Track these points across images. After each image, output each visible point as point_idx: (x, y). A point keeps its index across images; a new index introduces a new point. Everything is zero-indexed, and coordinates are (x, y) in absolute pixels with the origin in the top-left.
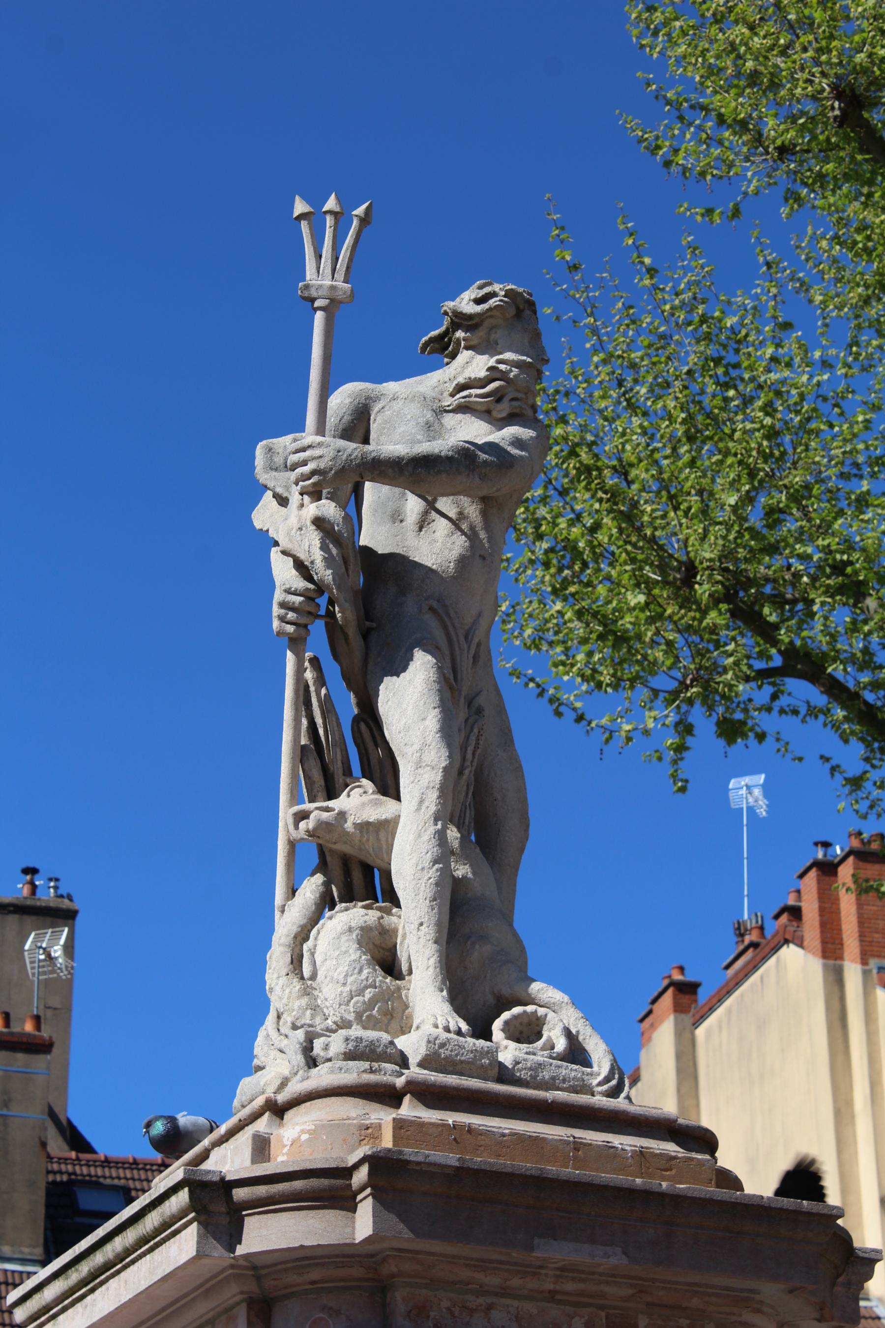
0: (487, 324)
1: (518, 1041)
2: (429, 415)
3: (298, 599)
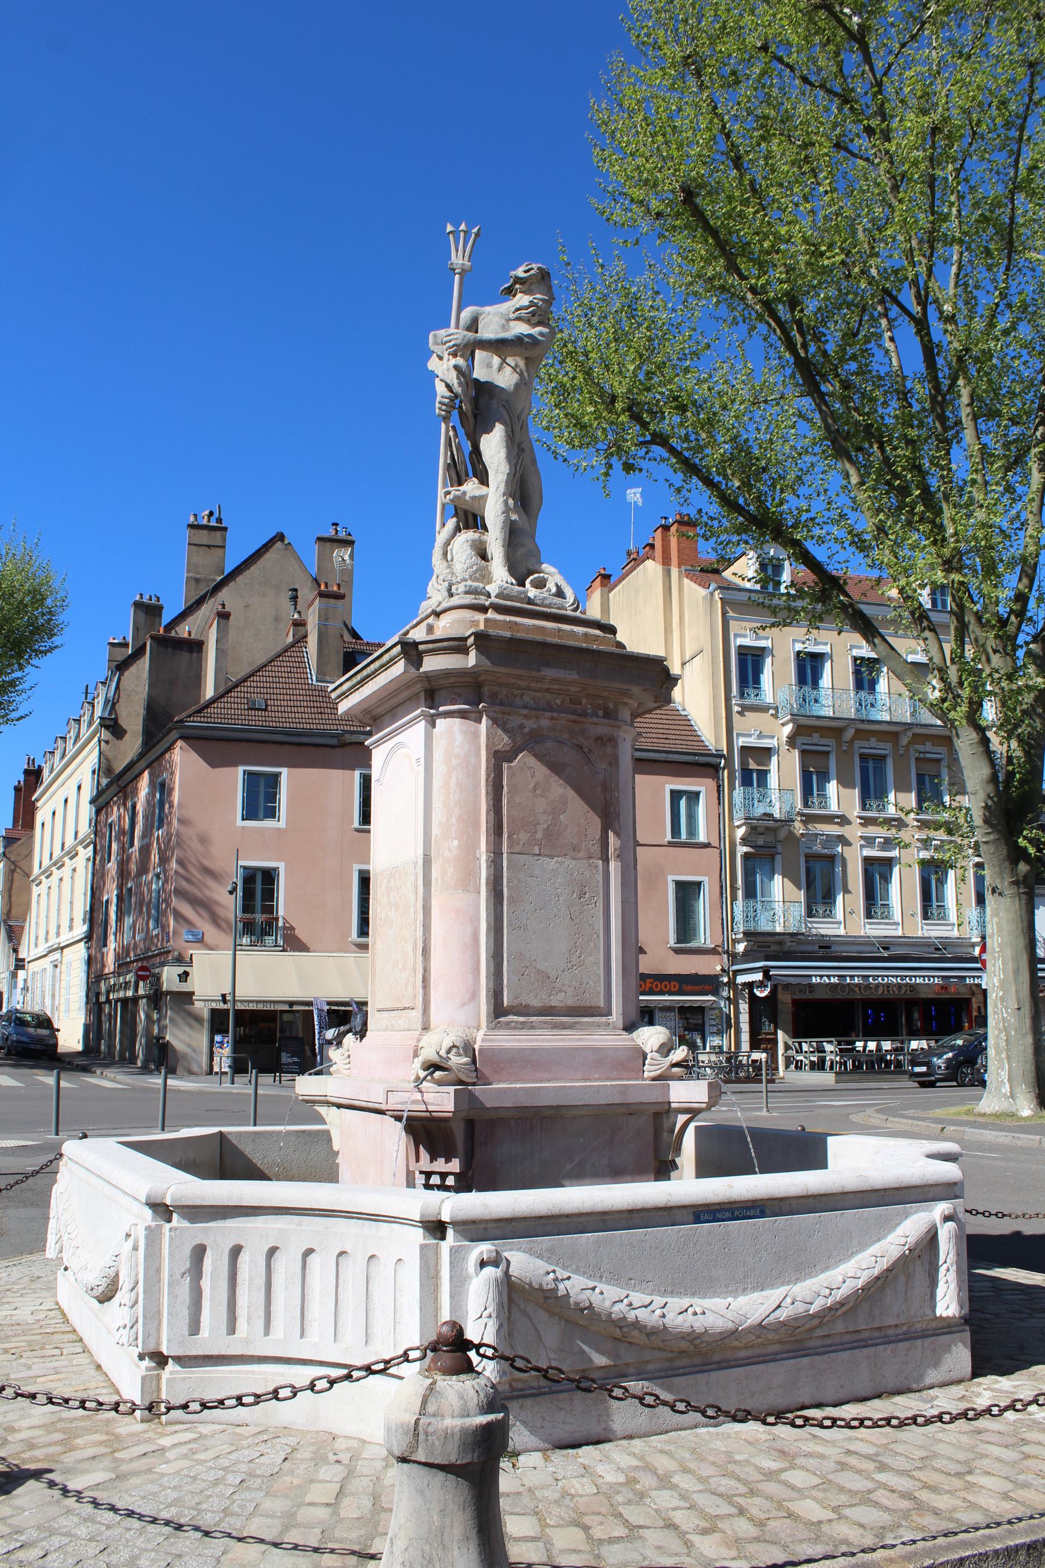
2: (504, 322)
3: (447, 401)
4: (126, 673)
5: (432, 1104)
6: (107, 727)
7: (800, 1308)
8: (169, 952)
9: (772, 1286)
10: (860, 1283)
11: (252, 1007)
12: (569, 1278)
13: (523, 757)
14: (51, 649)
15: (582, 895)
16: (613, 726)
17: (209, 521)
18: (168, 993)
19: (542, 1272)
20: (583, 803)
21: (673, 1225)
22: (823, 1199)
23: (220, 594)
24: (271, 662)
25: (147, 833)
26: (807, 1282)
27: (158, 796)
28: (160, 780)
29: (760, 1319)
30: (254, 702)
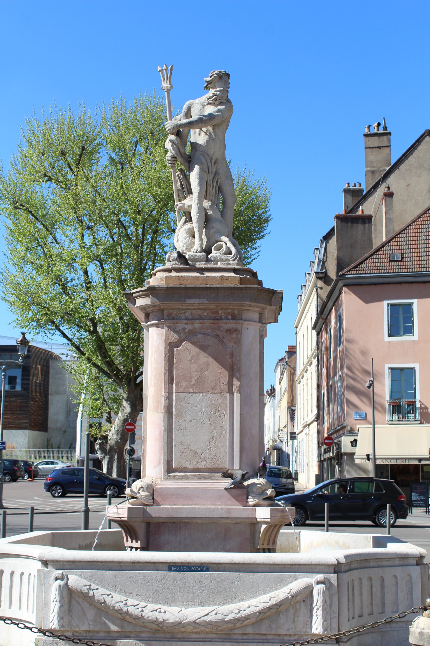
0: (213, 82)
1: (218, 251)
2: (201, 107)
4: (330, 241)
5: (121, 514)
6: (320, 278)
7: (219, 617)
8: (345, 427)
9: (209, 605)
10: (257, 609)
11: (393, 462)
12: (97, 589)
13: (186, 345)
14: (263, 236)
15: (217, 411)
16: (236, 323)
17: (378, 130)
18: (345, 454)
19: (82, 585)
20: (218, 365)
21: (157, 571)
22: (244, 566)
23: (389, 179)
24: (408, 227)
25: (335, 350)
26: (230, 605)
27: (338, 324)
28: (339, 313)
29: (194, 619)
30: (394, 257)
